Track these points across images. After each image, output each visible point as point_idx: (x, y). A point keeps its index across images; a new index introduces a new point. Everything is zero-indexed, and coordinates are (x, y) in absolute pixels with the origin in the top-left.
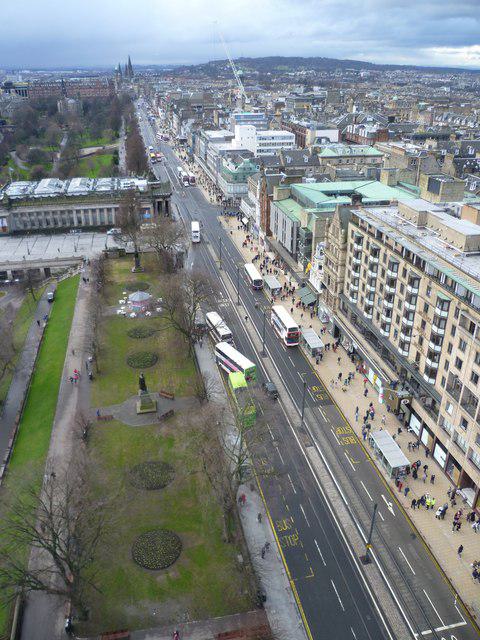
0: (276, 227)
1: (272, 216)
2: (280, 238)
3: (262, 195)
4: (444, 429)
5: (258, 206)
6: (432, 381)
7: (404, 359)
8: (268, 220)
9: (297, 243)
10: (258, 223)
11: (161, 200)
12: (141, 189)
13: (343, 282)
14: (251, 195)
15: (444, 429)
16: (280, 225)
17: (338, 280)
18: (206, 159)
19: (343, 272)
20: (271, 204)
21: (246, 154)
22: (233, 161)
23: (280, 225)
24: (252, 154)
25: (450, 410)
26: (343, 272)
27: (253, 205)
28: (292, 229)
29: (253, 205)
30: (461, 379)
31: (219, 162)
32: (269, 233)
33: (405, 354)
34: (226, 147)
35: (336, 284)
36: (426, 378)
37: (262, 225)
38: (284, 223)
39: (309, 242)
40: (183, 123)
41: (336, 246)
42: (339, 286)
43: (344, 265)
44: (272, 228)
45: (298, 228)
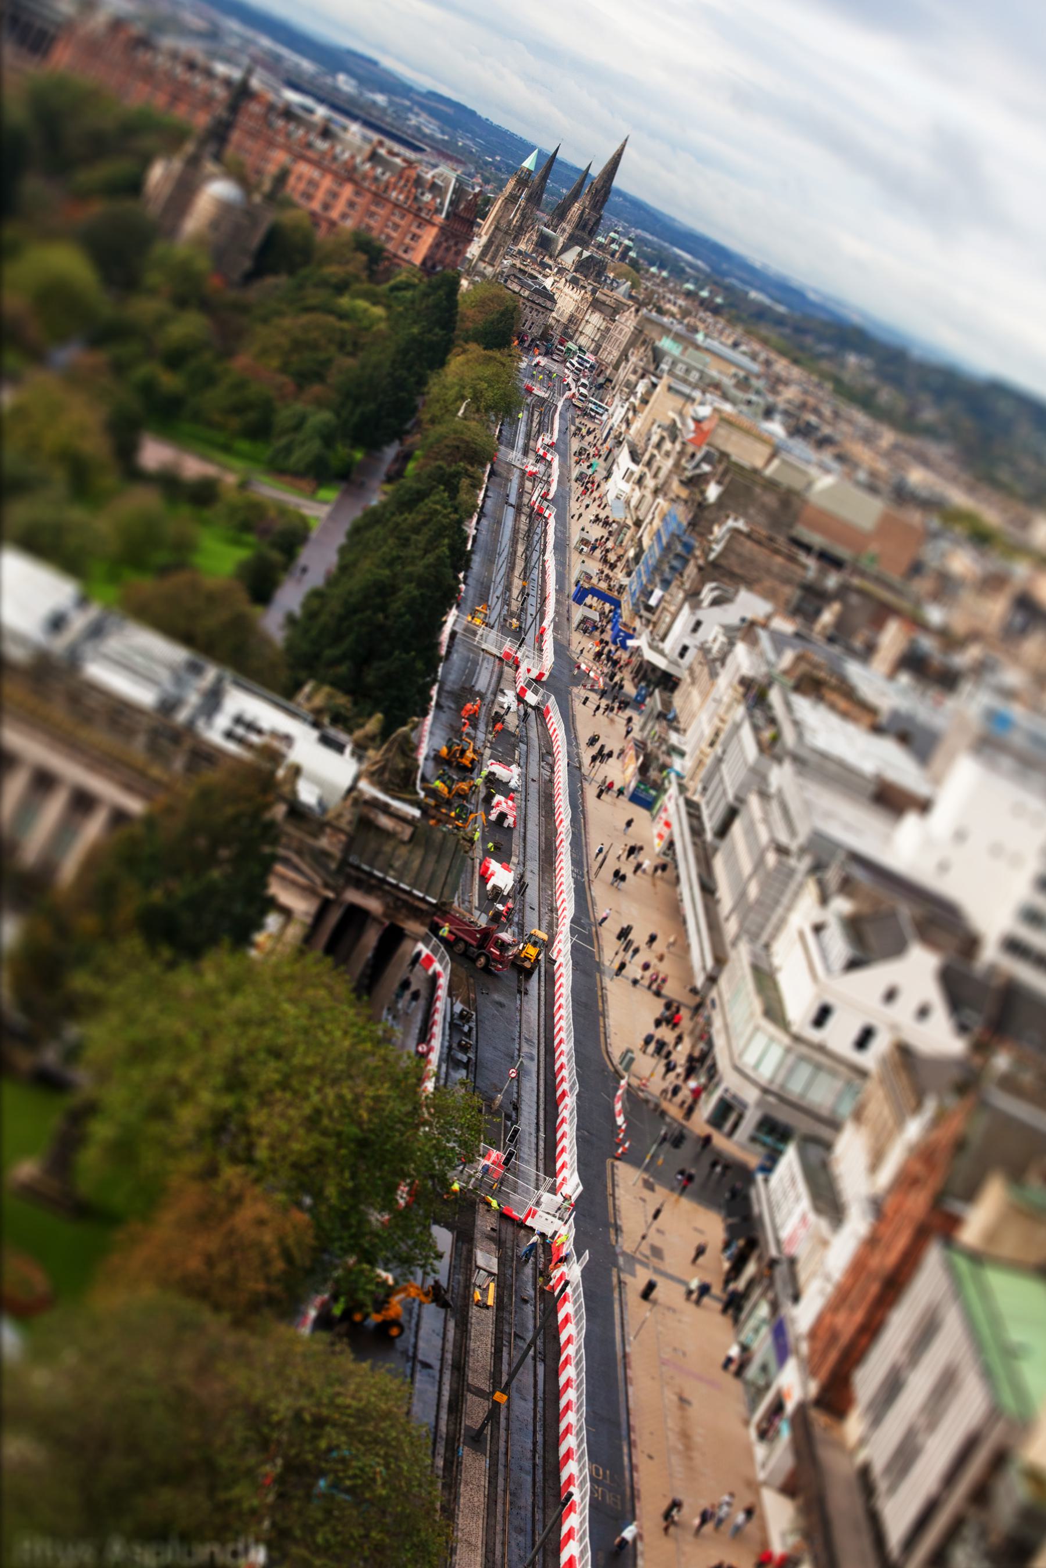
0: (893, 1387)
3: (905, 1181)
5: (858, 1223)
8: (871, 1330)
10: (803, 1316)
11: (373, 904)
12: (307, 794)
14: (850, 1151)
16: (919, 1385)
18: (723, 831)
20: (933, 1257)
21: (940, 921)
22: (854, 926)
23: (919, 1385)
24: (971, 944)
27: (828, 1201)
29: (828, 1201)
31: (777, 885)
32: (835, 1397)
34: (858, 829)
44: (867, 1381)
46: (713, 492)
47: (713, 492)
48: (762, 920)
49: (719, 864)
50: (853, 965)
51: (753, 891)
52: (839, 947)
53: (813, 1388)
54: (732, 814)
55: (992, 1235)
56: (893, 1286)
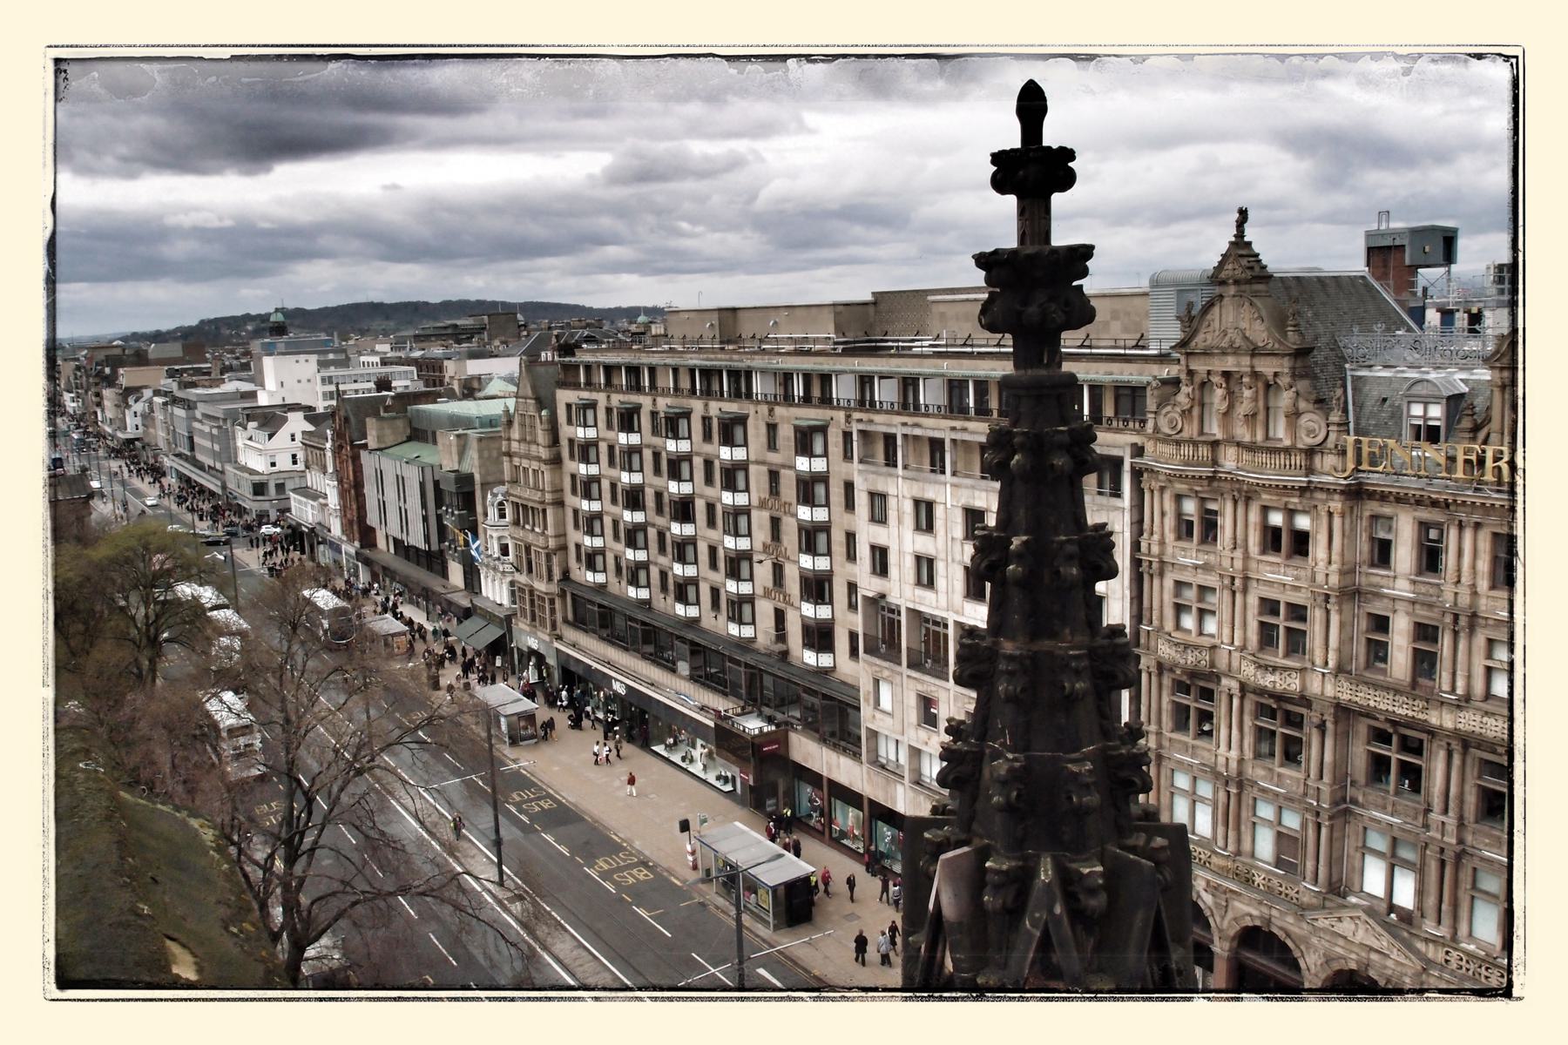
0: (383, 507)
1: (370, 491)
2: (394, 529)
4: (883, 767)
6: (826, 660)
7: (745, 645)
8: (362, 508)
9: (439, 518)
10: (336, 529)
13: (563, 548)
14: (315, 480)
15: (883, 767)
17: (552, 543)
19: (561, 523)
20: (364, 456)
25: (886, 703)
26: (561, 523)
28: (422, 485)
30: (893, 599)
33: (747, 632)
35: (548, 557)
36: (810, 658)
37: (347, 528)
38: (401, 481)
39: (467, 499)
40: (131, 401)
41: (535, 465)
42: (555, 560)
43: (560, 503)
44: (372, 519)
45: (436, 484)
46: (107, 370)
47: (107, 370)
48: (229, 454)
49: (200, 457)
50: (271, 436)
51: (217, 448)
52: (263, 435)
53: (357, 544)
54: (191, 439)
55: (380, 439)
56: (358, 485)
